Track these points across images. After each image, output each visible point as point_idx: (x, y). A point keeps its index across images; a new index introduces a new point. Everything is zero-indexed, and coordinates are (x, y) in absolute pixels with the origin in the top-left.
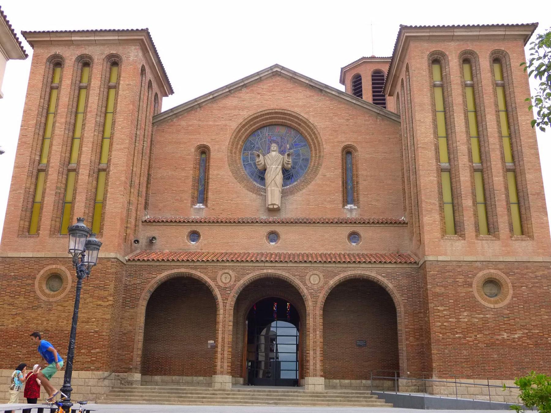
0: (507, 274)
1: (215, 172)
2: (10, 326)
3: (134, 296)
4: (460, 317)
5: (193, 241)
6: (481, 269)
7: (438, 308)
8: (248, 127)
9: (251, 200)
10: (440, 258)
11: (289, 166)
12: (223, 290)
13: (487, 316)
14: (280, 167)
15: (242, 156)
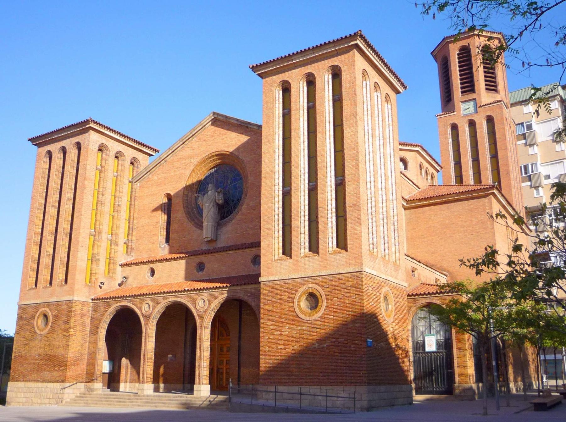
0: (322, 287)
1: (175, 215)
2: (23, 352)
4: (283, 330)
6: (302, 285)
7: (267, 323)
10: (271, 278)
11: (221, 201)
13: (303, 328)
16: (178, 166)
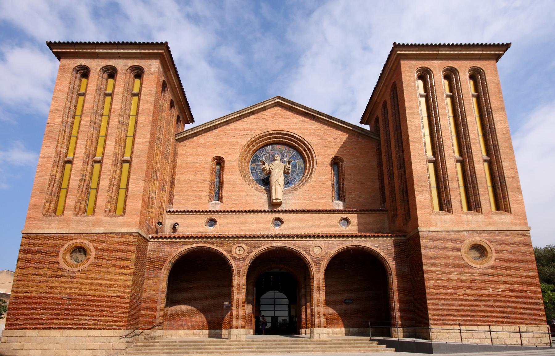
1: (229, 177)
3: (157, 266)
4: (451, 276)
5: (211, 226)
8: (255, 144)
9: (257, 197)
12: (237, 260)
13: (474, 274)
14: (282, 171)
15: (250, 167)
16: (231, 135)
